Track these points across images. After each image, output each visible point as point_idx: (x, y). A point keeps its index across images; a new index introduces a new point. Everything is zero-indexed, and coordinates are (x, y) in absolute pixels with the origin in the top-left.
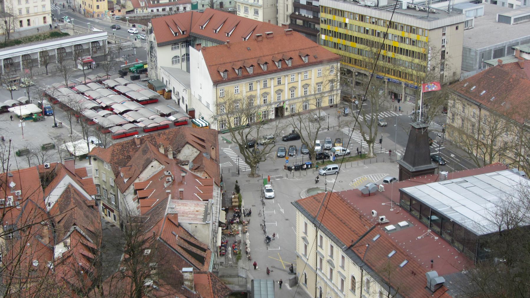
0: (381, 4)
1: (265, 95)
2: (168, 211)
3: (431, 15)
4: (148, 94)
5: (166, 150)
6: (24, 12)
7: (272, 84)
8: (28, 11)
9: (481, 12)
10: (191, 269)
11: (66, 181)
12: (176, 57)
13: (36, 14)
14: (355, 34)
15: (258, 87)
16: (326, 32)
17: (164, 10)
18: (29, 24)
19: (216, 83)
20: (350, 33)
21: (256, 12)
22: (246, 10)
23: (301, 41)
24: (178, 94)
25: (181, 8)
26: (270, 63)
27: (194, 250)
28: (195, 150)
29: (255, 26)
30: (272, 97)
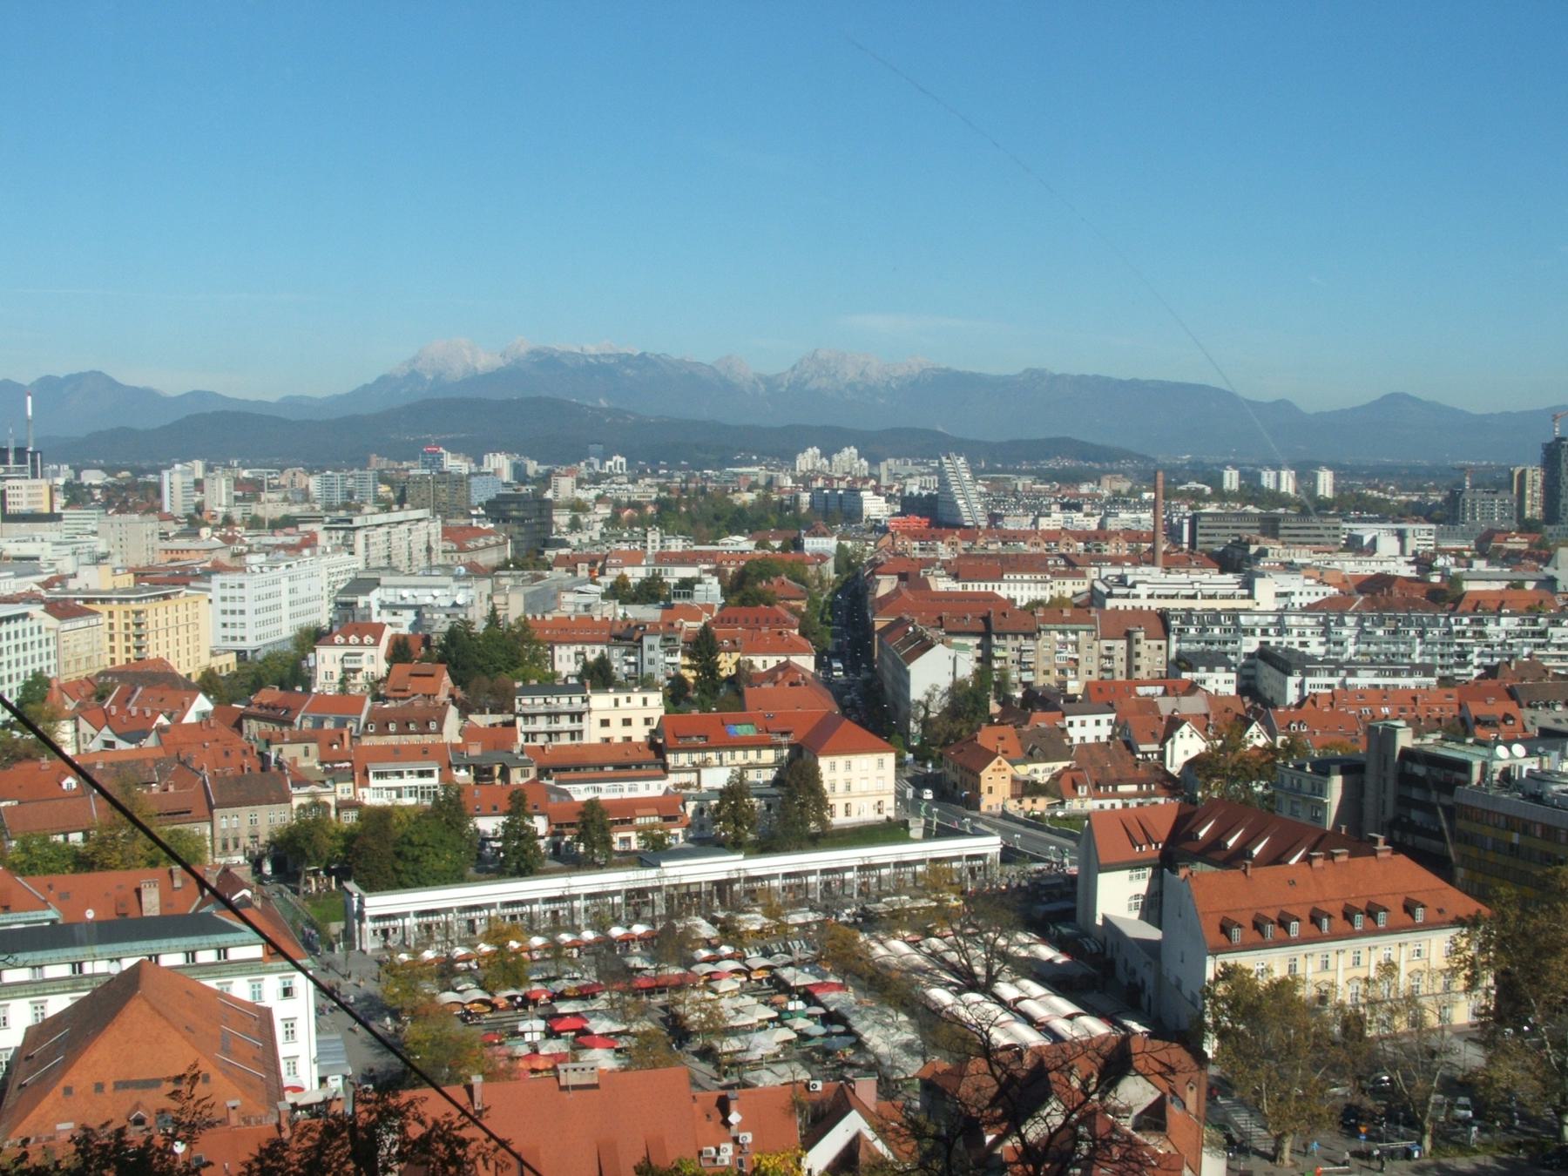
6: (840, 787)
8: (848, 788)
12: (1137, 896)
13: (864, 795)
17: (1125, 806)
18: (847, 813)
28: (1151, 1088)
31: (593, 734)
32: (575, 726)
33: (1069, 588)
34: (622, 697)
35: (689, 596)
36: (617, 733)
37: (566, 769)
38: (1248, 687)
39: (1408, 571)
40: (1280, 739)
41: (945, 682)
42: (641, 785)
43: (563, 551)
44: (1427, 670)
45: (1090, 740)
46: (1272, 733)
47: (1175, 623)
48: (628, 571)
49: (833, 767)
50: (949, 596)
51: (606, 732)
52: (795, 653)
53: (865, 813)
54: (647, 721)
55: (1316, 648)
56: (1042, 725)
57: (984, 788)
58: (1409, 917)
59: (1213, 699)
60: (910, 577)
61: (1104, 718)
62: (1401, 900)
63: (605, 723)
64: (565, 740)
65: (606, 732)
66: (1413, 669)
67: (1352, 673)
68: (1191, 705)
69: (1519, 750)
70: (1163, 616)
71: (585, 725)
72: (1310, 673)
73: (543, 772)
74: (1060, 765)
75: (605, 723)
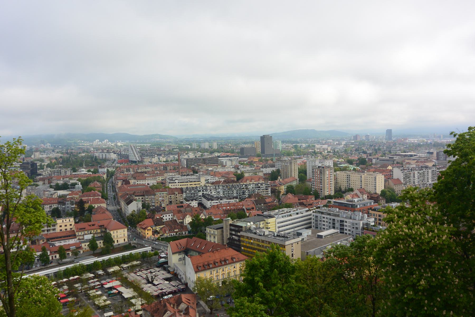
0: (265, 234)
1: (217, 276)
5: (174, 305)
6: (116, 237)
13: (121, 238)
14: (256, 247)
15: (214, 273)
16: (243, 246)
17: (176, 234)
19: (196, 272)
20: (253, 246)
21: (214, 237)
22: (210, 236)
23: (231, 252)
24: (181, 276)
25: (184, 233)
26: (219, 262)
30: (221, 277)
31: (58, 229)
32: (54, 228)
33: (160, 179)
34: (64, 220)
35: (74, 188)
36: (63, 228)
37: (54, 238)
38: (200, 204)
39: (233, 170)
40: (207, 217)
42: (71, 240)
44: (236, 198)
45: (168, 220)
46: (205, 216)
47: (184, 190)
48: (59, 182)
49: (114, 233)
50: (134, 185)
51: (61, 228)
52: (101, 203)
53: (121, 241)
54: (71, 225)
56: (158, 217)
57: (146, 234)
58: (233, 261)
59: (192, 208)
60: (126, 182)
61: (170, 215)
62: (231, 257)
63: (61, 226)
64: (52, 232)
65: (61, 228)
66: (234, 198)
67: (221, 200)
69: (252, 223)
70: (182, 189)
71: (56, 227)
72: (212, 200)
73: (48, 240)
74: (162, 226)
75: (61, 226)
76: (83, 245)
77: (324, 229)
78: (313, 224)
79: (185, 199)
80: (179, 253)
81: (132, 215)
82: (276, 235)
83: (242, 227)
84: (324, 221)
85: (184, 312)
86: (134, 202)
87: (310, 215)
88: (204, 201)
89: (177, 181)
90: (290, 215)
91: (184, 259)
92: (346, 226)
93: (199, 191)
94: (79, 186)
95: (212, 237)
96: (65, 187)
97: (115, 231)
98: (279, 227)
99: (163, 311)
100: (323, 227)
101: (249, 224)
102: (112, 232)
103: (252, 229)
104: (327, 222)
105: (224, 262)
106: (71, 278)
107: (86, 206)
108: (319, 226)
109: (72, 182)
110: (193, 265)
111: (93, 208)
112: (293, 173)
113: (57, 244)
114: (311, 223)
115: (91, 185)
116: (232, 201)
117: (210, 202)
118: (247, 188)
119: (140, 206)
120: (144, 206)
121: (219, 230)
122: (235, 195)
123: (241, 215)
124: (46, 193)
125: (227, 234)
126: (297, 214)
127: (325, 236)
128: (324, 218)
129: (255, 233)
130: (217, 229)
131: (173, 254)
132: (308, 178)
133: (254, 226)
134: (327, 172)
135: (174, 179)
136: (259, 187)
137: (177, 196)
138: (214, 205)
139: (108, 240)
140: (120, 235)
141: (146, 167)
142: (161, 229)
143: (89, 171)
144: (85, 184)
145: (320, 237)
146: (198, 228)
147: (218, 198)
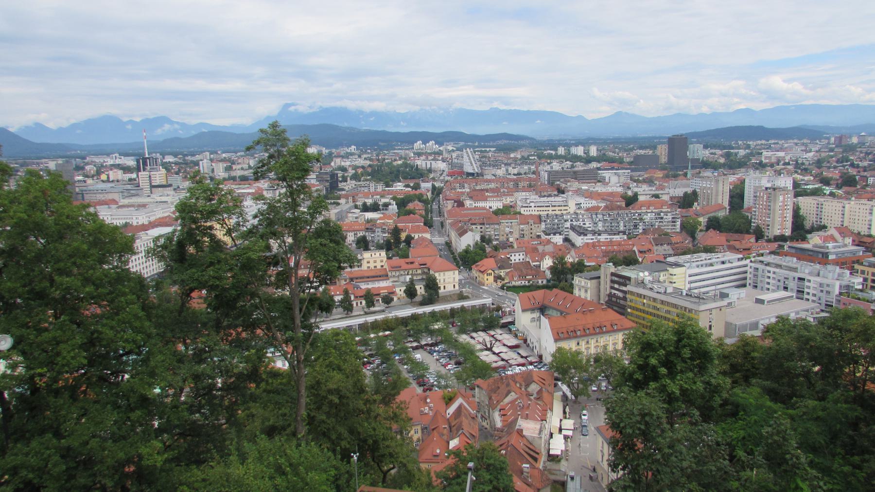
2: (517, 427)
3: (701, 301)
4: (513, 342)
5: (521, 385)
6: (442, 281)
7: (593, 342)
9: (743, 295)
10: (528, 466)
11: (459, 401)
13: (449, 283)
14: (650, 310)
16: (630, 307)
19: (556, 340)
20: (647, 309)
21: (586, 291)
22: (580, 290)
23: (612, 315)
25: (540, 281)
26: (591, 329)
27: (532, 453)
29: (584, 303)
33: (508, 200)
38: (566, 240)
39: (620, 190)
40: (577, 259)
41: (472, 244)
43: (343, 192)
44: (624, 233)
45: (517, 261)
47: (543, 219)
48: (366, 200)
52: (424, 232)
53: (450, 288)
55: (588, 224)
59: (555, 245)
63: (368, 262)
67: (599, 235)
68: (549, 248)
72: (586, 235)
73: (352, 280)
75: (368, 262)
76: (397, 290)
77: (768, 289)
78: (748, 281)
79: (544, 232)
80: (532, 310)
81: (467, 251)
82: (684, 294)
83: (629, 279)
84: (769, 277)
85: (535, 395)
86: (469, 233)
87: (746, 266)
88: (573, 236)
89: (532, 205)
90: (711, 265)
91: (539, 319)
92: (809, 287)
93: (566, 221)
94: (394, 208)
95: (583, 291)
96: (375, 208)
97: (442, 274)
98: (690, 282)
99: (505, 392)
100: (768, 286)
101: (641, 274)
102: (437, 275)
103: (646, 281)
104: (774, 278)
105: (599, 330)
106: (381, 334)
107: (403, 236)
108: (759, 285)
109: (384, 200)
110: (552, 329)
111: (413, 238)
112: (720, 197)
113: (364, 286)
114: (745, 279)
115: (410, 206)
116: (616, 238)
117: (582, 237)
118: (641, 219)
119: (478, 238)
120: (483, 238)
121: (594, 281)
122: (622, 229)
123: (630, 261)
124: (350, 215)
125: (606, 287)
126: (723, 263)
127: (768, 302)
128: (769, 272)
129: (651, 289)
130: (591, 279)
131: (524, 311)
132: (746, 205)
133: (650, 278)
134: (781, 198)
135: (528, 201)
136: (662, 218)
137: (533, 227)
138: (588, 243)
139: (432, 286)
140: (449, 280)
141: (490, 181)
142: (507, 274)
143: (407, 186)
144: (402, 204)
145: (760, 301)
146: (562, 275)
147: (594, 233)
